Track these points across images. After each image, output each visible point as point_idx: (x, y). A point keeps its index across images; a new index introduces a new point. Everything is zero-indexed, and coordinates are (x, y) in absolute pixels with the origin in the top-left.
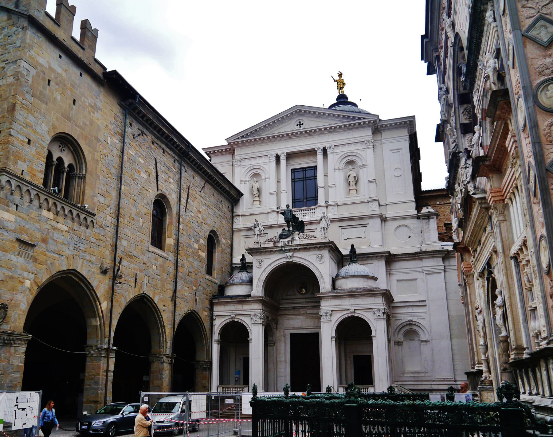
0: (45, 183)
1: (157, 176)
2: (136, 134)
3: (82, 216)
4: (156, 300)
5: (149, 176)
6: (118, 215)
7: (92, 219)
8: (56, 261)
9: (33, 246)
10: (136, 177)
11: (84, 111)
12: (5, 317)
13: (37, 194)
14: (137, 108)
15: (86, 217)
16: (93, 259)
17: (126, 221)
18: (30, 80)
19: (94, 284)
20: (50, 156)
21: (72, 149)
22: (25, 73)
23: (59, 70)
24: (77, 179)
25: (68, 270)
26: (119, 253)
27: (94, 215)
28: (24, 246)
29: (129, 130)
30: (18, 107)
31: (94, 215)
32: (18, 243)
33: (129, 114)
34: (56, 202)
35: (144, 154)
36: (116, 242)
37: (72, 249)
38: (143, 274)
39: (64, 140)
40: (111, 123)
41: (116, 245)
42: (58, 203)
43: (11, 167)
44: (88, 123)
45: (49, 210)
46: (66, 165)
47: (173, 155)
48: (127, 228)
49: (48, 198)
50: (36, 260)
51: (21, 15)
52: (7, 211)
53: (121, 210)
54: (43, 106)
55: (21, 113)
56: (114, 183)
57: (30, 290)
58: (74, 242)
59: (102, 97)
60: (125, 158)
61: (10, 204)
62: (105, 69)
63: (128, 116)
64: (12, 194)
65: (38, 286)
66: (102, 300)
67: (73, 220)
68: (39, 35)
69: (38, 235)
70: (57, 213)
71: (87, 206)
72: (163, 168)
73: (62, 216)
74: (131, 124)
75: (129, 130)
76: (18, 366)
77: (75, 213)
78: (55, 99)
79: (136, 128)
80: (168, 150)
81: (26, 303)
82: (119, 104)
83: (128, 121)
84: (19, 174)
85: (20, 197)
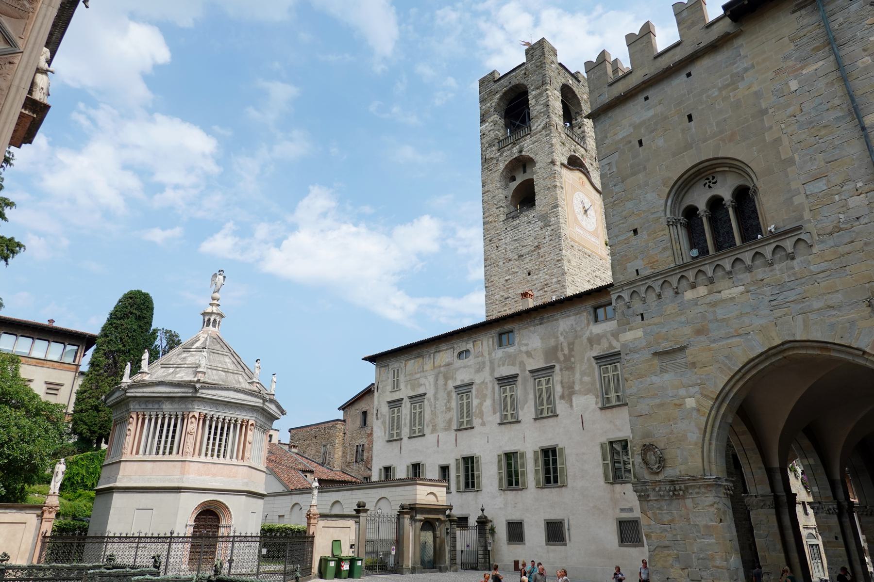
9: (682, 349)
21: (727, 169)
39: (704, 172)
50: (694, 365)
52: (630, 330)
57: (698, 410)
58: (768, 299)
67: (749, 269)
69: (687, 330)
73: (723, 278)
76: (707, 527)
84: (633, 276)
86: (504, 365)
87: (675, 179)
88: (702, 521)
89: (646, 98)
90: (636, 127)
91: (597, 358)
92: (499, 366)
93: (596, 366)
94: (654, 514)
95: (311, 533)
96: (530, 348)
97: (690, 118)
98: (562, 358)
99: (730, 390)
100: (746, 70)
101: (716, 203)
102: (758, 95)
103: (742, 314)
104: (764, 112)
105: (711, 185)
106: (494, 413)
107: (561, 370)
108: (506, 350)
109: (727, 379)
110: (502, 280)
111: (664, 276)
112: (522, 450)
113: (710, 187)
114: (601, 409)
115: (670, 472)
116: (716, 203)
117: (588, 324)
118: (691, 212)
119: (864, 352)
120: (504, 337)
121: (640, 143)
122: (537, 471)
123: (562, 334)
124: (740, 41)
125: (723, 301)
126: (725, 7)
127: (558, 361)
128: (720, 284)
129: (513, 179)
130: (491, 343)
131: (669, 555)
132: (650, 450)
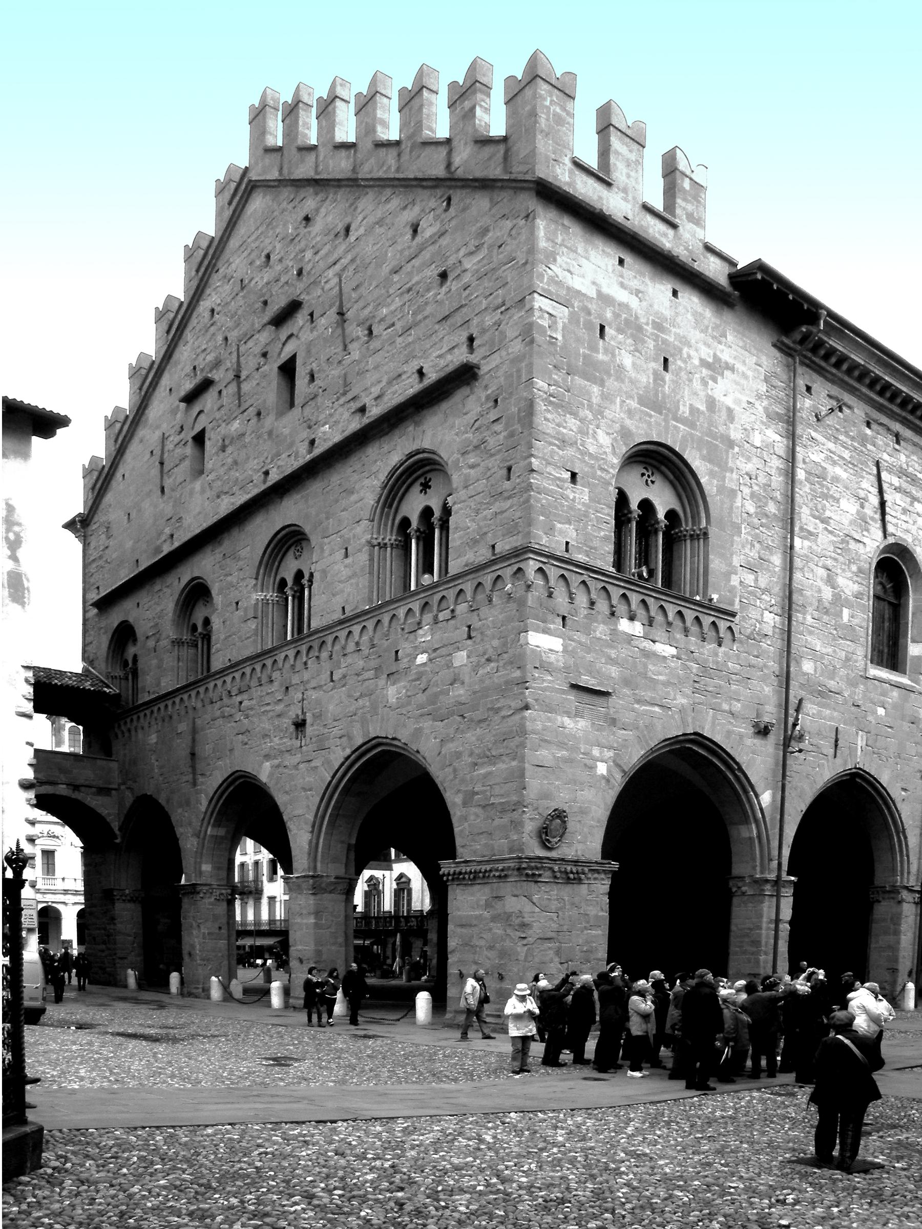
0: (619, 563)
1: (883, 504)
2: (824, 411)
3: (707, 621)
5: (862, 506)
6: (789, 606)
7: (728, 624)
8: (655, 720)
10: (828, 514)
11: (690, 380)
12: (564, 833)
13: (604, 588)
15: (716, 619)
17: (809, 617)
18: (560, 337)
19: (742, 758)
20: (622, 499)
21: (672, 477)
22: (545, 323)
23: (622, 296)
24: (688, 542)
25: (684, 735)
26: (795, 692)
27: (733, 615)
28: (587, 698)
29: (806, 404)
30: (541, 406)
31: (733, 615)
32: (574, 692)
33: (802, 363)
34: (646, 598)
35: (846, 454)
36: (788, 666)
40: (759, 397)
41: (788, 673)
42: (650, 601)
43: (543, 540)
44: (703, 408)
45: (632, 618)
46: (661, 515)
48: (811, 633)
49: (628, 593)
50: (613, 722)
51: (516, 185)
53: (795, 597)
54: (595, 389)
55: (549, 416)
56: (773, 535)
57: (608, 781)
59: (730, 338)
60: (801, 474)
61: (550, 617)
62: (732, 263)
63: (800, 370)
64: (550, 595)
65: (624, 771)
67: (686, 631)
70: (650, 622)
71: (715, 597)
72: (896, 481)
73: (661, 625)
74: (809, 389)
75: (806, 404)
77: (689, 615)
78: (621, 367)
79: (824, 393)
80: (907, 433)
81: (602, 806)
82: (774, 345)
83: (801, 383)
84: (560, 552)
85: (567, 600)
105: (645, 477)
118: (622, 499)
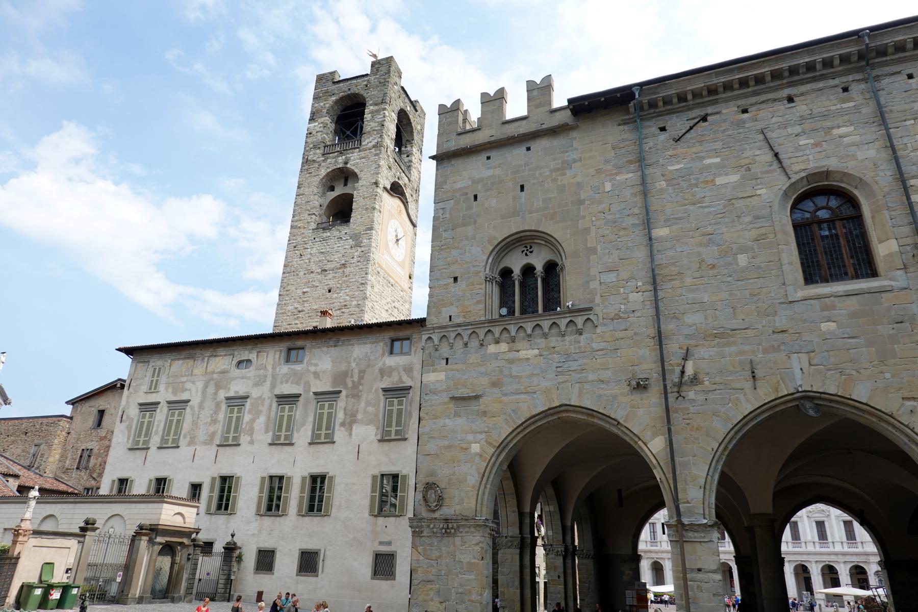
4: (861, 393)
9: (477, 397)
14: (652, 105)
16: (607, 374)
37: (552, 376)
38: (783, 355)
39: (523, 240)
47: (832, 82)
50: (484, 413)
52: (433, 371)
57: (481, 456)
58: (555, 365)
66: (646, 436)
67: (545, 336)
68: (453, 162)
69: (485, 381)
73: (523, 339)
76: (469, 563)
81: (477, 475)
84: (446, 321)
86: (287, 382)
87: (500, 240)
88: (466, 558)
89: (488, 158)
90: (475, 182)
91: (385, 390)
92: (281, 383)
93: (382, 398)
94: (425, 550)
95: (16, 553)
96: (319, 369)
97: (522, 188)
98: (350, 385)
99: (511, 441)
100: (575, 161)
101: (528, 270)
102: (579, 185)
103: (532, 375)
104: (581, 202)
106: (267, 432)
107: (347, 396)
108: (292, 367)
109: (510, 430)
110: (299, 292)
111: (473, 327)
112: (289, 474)
113: (526, 255)
114: (380, 441)
115: (445, 512)
116: (528, 270)
117: (383, 355)
118: (506, 273)
119: (619, 423)
120: (293, 353)
121: (476, 197)
122: (301, 498)
123: (354, 360)
124: (574, 134)
125: (520, 360)
126: (570, 101)
127: (346, 387)
128: (520, 344)
129: (332, 189)
130: (277, 356)
131: (431, 589)
132: (431, 488)
